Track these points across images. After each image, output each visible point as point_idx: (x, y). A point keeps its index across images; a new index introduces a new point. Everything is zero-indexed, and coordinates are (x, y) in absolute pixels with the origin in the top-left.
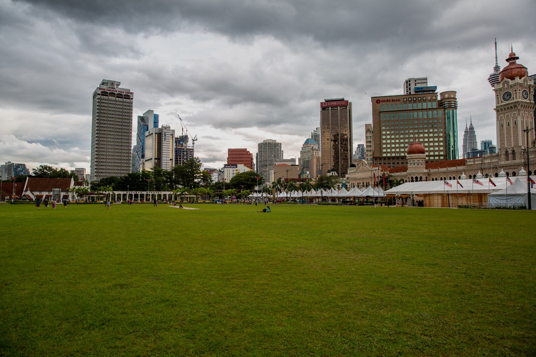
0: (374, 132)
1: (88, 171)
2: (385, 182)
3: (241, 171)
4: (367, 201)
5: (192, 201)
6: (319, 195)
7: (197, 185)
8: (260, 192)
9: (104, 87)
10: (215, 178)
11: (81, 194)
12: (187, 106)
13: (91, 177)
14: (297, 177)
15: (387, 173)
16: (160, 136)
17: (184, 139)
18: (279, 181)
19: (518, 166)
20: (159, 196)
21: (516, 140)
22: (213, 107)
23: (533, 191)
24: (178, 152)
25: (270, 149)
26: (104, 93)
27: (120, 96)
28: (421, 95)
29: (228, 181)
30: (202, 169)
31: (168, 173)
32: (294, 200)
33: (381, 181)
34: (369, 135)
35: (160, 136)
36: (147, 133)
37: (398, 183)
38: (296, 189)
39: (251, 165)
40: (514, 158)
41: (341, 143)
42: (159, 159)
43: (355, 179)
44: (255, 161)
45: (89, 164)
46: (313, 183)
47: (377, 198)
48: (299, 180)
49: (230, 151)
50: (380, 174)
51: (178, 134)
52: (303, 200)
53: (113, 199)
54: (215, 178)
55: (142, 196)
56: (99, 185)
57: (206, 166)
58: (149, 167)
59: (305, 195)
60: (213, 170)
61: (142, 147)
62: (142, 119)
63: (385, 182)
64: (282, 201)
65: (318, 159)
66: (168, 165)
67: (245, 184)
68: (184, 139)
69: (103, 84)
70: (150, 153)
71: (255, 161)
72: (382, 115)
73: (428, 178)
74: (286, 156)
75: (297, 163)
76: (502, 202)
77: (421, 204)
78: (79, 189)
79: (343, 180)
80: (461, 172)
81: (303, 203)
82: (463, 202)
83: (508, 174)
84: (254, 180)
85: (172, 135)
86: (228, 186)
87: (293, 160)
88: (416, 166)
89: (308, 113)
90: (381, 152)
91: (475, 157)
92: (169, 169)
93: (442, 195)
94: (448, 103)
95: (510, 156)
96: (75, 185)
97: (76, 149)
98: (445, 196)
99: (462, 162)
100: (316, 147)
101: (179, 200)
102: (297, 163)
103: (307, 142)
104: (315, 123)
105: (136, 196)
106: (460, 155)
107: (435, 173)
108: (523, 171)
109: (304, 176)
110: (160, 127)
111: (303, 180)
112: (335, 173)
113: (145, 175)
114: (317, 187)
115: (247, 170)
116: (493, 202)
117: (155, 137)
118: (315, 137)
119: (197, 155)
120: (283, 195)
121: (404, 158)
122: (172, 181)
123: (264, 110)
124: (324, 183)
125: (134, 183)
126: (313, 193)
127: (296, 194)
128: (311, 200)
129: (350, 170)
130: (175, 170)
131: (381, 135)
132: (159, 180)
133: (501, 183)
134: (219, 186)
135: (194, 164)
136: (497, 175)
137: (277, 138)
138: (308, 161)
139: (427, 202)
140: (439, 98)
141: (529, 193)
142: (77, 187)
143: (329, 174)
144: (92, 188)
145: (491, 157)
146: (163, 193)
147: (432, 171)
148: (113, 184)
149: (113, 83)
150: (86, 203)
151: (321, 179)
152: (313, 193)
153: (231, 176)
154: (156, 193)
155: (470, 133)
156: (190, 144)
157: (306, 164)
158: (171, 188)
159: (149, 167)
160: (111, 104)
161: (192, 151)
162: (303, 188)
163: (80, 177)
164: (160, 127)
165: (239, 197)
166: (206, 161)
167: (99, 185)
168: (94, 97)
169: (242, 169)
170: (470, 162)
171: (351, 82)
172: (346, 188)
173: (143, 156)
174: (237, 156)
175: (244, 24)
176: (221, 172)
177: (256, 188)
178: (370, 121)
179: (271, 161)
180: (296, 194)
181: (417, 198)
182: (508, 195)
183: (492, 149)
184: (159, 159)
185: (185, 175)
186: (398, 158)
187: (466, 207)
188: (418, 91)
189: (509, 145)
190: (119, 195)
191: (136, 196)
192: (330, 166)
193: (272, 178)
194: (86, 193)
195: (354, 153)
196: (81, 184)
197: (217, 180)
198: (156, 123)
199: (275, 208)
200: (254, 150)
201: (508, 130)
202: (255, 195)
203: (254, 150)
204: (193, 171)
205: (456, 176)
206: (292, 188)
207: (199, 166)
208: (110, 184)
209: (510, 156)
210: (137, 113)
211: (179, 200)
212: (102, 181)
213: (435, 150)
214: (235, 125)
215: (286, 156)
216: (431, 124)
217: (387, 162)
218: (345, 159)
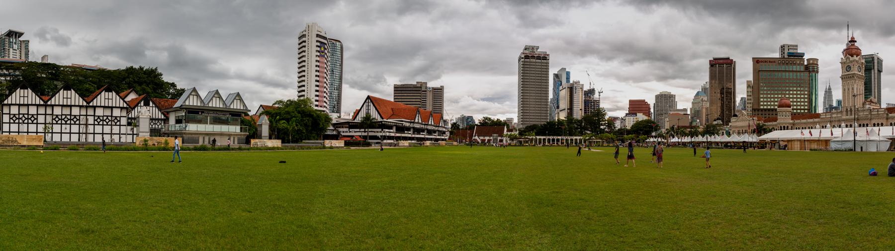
1: (516, 121)
3: (640, 120)
4: (745, 146)
7: (602, 131)
8: (655, 137)
10: (618, 125)
13: (518, 125)
14: (688, 125)
15: (761, 123)
16: (571, 90)
17: (591, 92)
18: (672, 128)
20: (572, 140)
22: (614, 65)
24: (586, 103)
25: (666, 100)
29: (629, 128)
30: (607, 117)
31: (579, 121)
35: (571, 90)
36: (561, 88)
37: (770, 131)
38: (686, 135)
39: (648, 113)
41: (727, 94)
42: (571, 109)
43: (736, 127)
44: (652, 110)
48: (691, 127)
49: (630, 101)
51: (586, 88)
54: (618, 125)
55: (558, 140)
57: (609, 115)
58: (563, 116)
59: (693, 140)
60: (616, 119)
62: (556, 76)
63: (760, 130)
64: (675, 145)
65: (707, 109)
66: (578, 113)
67: (644, 130)
68: (591, 92)
70: (564, 104)
71: (652, 110)
74: (680, 106)
75: (689, 112)
79: (727, 128)
80: (815, 123)
84: (651, 127)
86: (629, 132)
87: (685, 110)
88: (784, 118)
92: (579, 118)
100: (706, 99)
102: (689, 112)
103: (698, 93)
105: (553, 140)
107: (798, 124)
109: (694, 124)
110: (571, 82)
111: (694, 127)
112: (720, 122)
113: (560, 122)
115: (646, 118)
118: (704, 89)
120: (676, 140)
122: (582, 128)
124: (710, 130)
125: (552, 129)
126: (700, 139)
127: (687, 139)
129: (733, 119)
130: (585, 118)
132: (571, 127)
133: (837, 132)
134: (622, 132)
135: (600, 114)
137: (672, 90)
138: (698, 111)
143: (715, 123)
146: (575, 138)
147: (796, 121)
151: (708, 127)
152: (700, 139)
153: (632, 123)
154: (569, 138)
156: (596, 96)
157: (696, 113)
158: (581, 134)
159: (563, 116)
161: (598, 102)
162: (692, 134)
164: (571, 82)
166: (610, 110)
169: (641, 117)
173: (558, 107)
174: (637, 106)
176: (623, 120)
177: (654, 134)
179: (666, 110)
180: (687, 139)
184: (571, 109)
185: (592, 122)
191: (553, 140)
193: (667, 126)
195: (737, 104)
198: (568, 79)
200: (651, 101)
202: (652, 140)
203: (651, 101)
204: (599, 119)
206: (685, 134)
207: (604, 115)
210: (552, 71)
212: (527, 128)
215: (680, 106)
218: (730, 110)
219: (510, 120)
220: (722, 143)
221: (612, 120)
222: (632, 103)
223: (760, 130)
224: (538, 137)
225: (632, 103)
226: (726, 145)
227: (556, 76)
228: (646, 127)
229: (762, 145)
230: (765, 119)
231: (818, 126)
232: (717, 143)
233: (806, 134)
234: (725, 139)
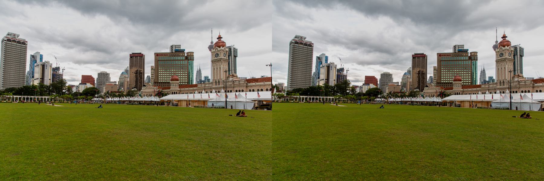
0: (438, 70)
1: (286, 85)
2: (442, 95)
4: (433, 104)
5: (344, 102)
6: (410, 100)
7: (348, 94)
9: (296, 39)
10: (358, 90)
11: (280, 97)
12: (345, 53)
18: (390, 93)
19: (505, 88)
20: (327, 99)
21: (505, 76)
23: (512, 101)
24: (338, 76)
25: (386, 77)
26: (296, 43)
27: (306, 44)
28: (460, 53)
32: (397, 102)
33: (440, 94)
34: (435, 71)
36: (321, 66)
40: (504, 85)
44: (379, 83)
45: (287, 81)
46: (407, 94)
47: (438, 102)
50: (440, 90)
52: (402, 102)
53: (300, 100)
54: (358, 90)
56: (291, 92)
58: (322, 83)
59: (403, 100)
61: (318, 74)
62: (319, 58)
63: (442, 95)
64: (392, 103)
69: (296, 37)
70: (323, 76)
71: (379, 83)
72: (442, 62)
73: (463, 93)
74: (394, 81)
76: (498, 106)
77: (459, 106)
78: (279, 94)
79: (422, 93)
81: (402, 104)
82: (479, 105)
83: (500, 92)
85: (336, 67)
86: (364, 95)
89: (406, 59)
90: (441, 80)
91: (485, 84)
93: (469, 101)
94: (473, 57)
95: (502, 84)
96: (277, 92)
97: (279, 72)
98: (471, 103)
99: (479, 86)
101: (337, 101)
104: (409, 65)
106: (478, 83)
107: (466, 91)
108: (508, 91)
109: (403, 91)
112: (418, 90)
114: (409, 96)
116: (494, 106)
117: (326, 68)
119: (348, 78)
121: (451, 83)
123: (384, 57)
124: (413, 94)
127: (398, 100)
128: (406, 102)
131: (441, 72)
134: (360, 94)
135: (346, 83)
136: (495, 93)
138: (405, 84)
139: (462, 105)
140: (469, 55)
141: (511, 102)
142: (277, 93)
144: (287, 94)
145: (493, 84)
146: (329, 97)
148: (300, 92)
149: (302, 38)
150: (282, 102)
154: (325, 97)
155: (483, 72)
160: (300, 49)
163: (280, 88)
164: (329, 63)
165: (370, 100)
167: (291, 92)
168: (290, 44)
169: (372, 86)
170: (483, 86)
171: (428, 44)
172: (423, 97)
173: (319, 78)
174: (369, 80)
175: (373, 10)
176: (361, 87)
178: (436, 65)
180: (398, 100)
181: (457, 103)
182: (501, 103)
183: (493, 80)
185: (341, 88)
186: (449, 83)
187: (481, 108)
188: (460, 51)
189: (502, 78)
190: (303, 98)
191: (313, 99)
192: (416, 86)
194: (283, 96)
196: (280, 91)
197: (358, 92)
199: (386, 106)
201: (501, 71)
203: (378, 77)
205: (476, 93)
207: (349, 84)
208: (298, 92)
209: (502, 84)
210: (315, 55)
211: (337, 101)
213: (467, 80)
214: (369, 63)
215: (394, 81)
216: (465, 67)
217: (443, 85)
219: (281, 85)
220: (419, 102)
221: (354, 88)
222: (367, 77)
223: (442, 95)
224: (301, 97)
225: (367, 77)
226: (422, 103)
227: (319, 58)
228: (374, 92)
229: (444, 104)
230: (445, 88)
231: (480, 92)
232: (417, 102)
233: (474, 97)
234: (422, 100)
